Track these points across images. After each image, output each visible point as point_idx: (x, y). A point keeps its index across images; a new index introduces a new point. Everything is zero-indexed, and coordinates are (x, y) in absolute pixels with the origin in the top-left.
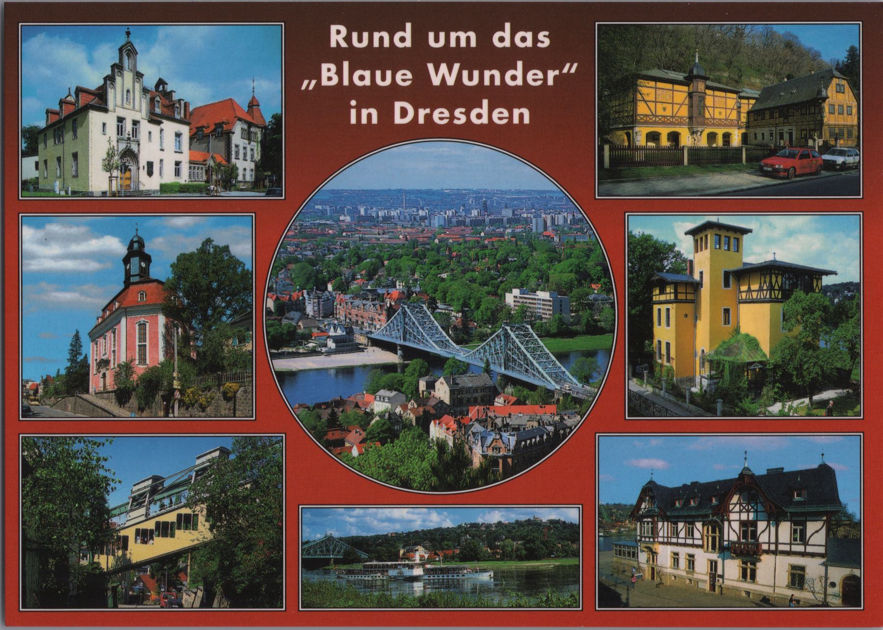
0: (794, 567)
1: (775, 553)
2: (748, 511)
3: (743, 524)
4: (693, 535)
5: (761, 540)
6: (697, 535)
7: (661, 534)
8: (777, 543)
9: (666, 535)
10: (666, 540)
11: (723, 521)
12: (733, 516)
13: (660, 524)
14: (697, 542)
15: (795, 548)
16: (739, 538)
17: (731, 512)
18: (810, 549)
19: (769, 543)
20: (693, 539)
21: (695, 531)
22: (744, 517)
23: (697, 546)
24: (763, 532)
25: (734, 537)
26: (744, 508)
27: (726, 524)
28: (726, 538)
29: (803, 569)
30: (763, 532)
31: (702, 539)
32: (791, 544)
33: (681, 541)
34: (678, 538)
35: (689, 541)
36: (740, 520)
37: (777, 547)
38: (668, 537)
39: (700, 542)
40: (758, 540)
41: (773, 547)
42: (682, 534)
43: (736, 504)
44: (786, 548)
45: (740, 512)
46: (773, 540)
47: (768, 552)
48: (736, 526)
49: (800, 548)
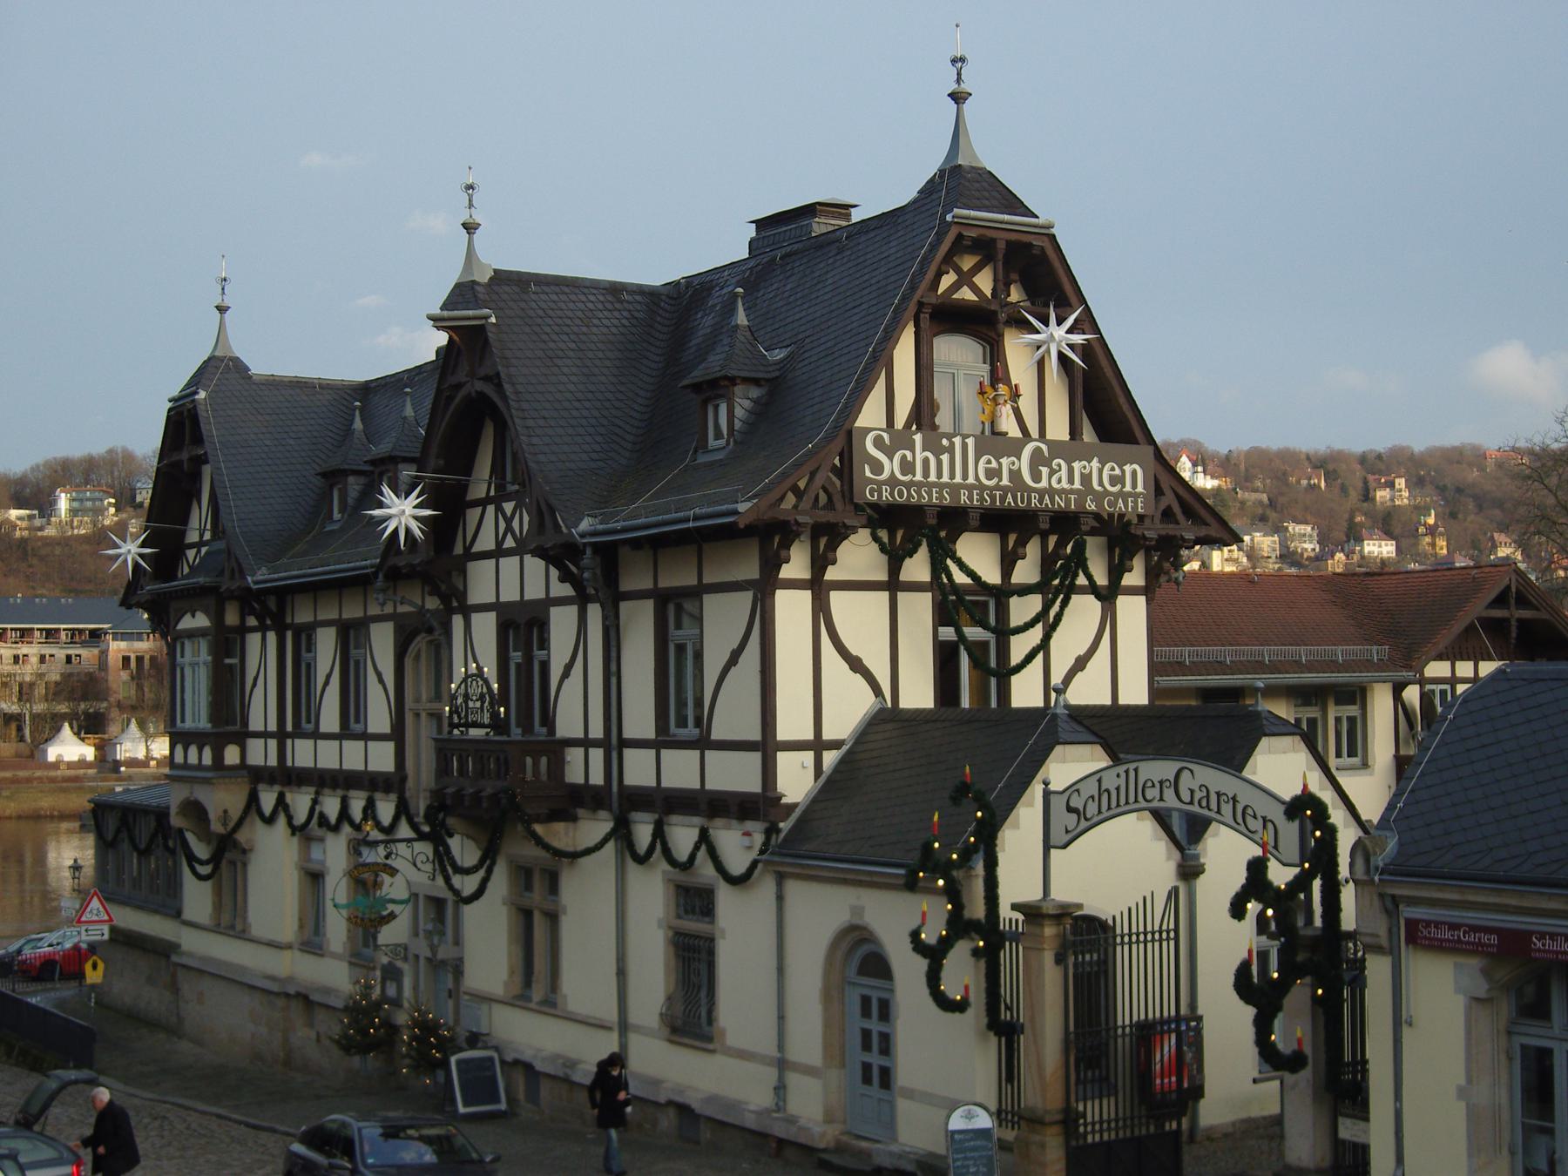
31: (397, 734)
38: (281, 736)
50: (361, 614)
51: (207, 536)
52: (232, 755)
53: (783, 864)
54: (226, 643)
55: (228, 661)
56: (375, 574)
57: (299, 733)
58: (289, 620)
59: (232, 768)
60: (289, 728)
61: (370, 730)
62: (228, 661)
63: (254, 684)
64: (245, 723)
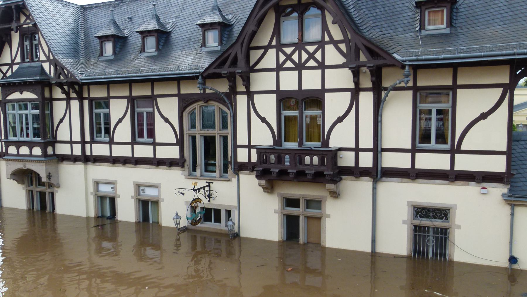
0: (421, 211)
1: (378, 174)
2: (300, 67)
3: (284, 99)
4: (151, 133)
5: (334, 143)
6: (164, 133)
7: (63, 134)
8: (377, 150)
9: (77, 137)
10: (77, 150)
11: (233, 92)
12: (263, 81)
13: (59, 108)
14: (163, 153)
15: (426, 161)
16: (277, 141)
17: (253, 69)
18: (463, 163)
19: (357, 150)
20: (154, 144)
21: (159, 124)
22: (289, 81)
23: (170, 163)
24: (340, 120)
25: (263, 138)
26: (289, 57)
27: (242, 101)
28: (242, 139)
29: (442, 213)
30: (340, 120)
31: (180, 142)
32: (414, 151)
33: (123, 151)
34: (111, 142)
35: (143, 151)
36: (278, 92)
37: (376, 160)
38: (83, 142)
39: (174, 153)
40: (326, 143)
41: (366, 160)
42: (123, 133)
43: (266, 49)
44: (402, 161)
45: (279, 68)
46: (366, 141)
47: (357, 172)
48: (267, 105)
49: (440, 162)
50: (149, 93)
51: (18, 60)
52: (50, 151)
53: (514, 201)
54: (46, 104)
55: (37, 112)
56: (197, 77)
57: (93, 141)
58: (86, 95)
59: (50, 156)
60: (88, 138)
61: (157, 141)
62: (37, 112)
63: (61, 121)
64: (54, 136)
